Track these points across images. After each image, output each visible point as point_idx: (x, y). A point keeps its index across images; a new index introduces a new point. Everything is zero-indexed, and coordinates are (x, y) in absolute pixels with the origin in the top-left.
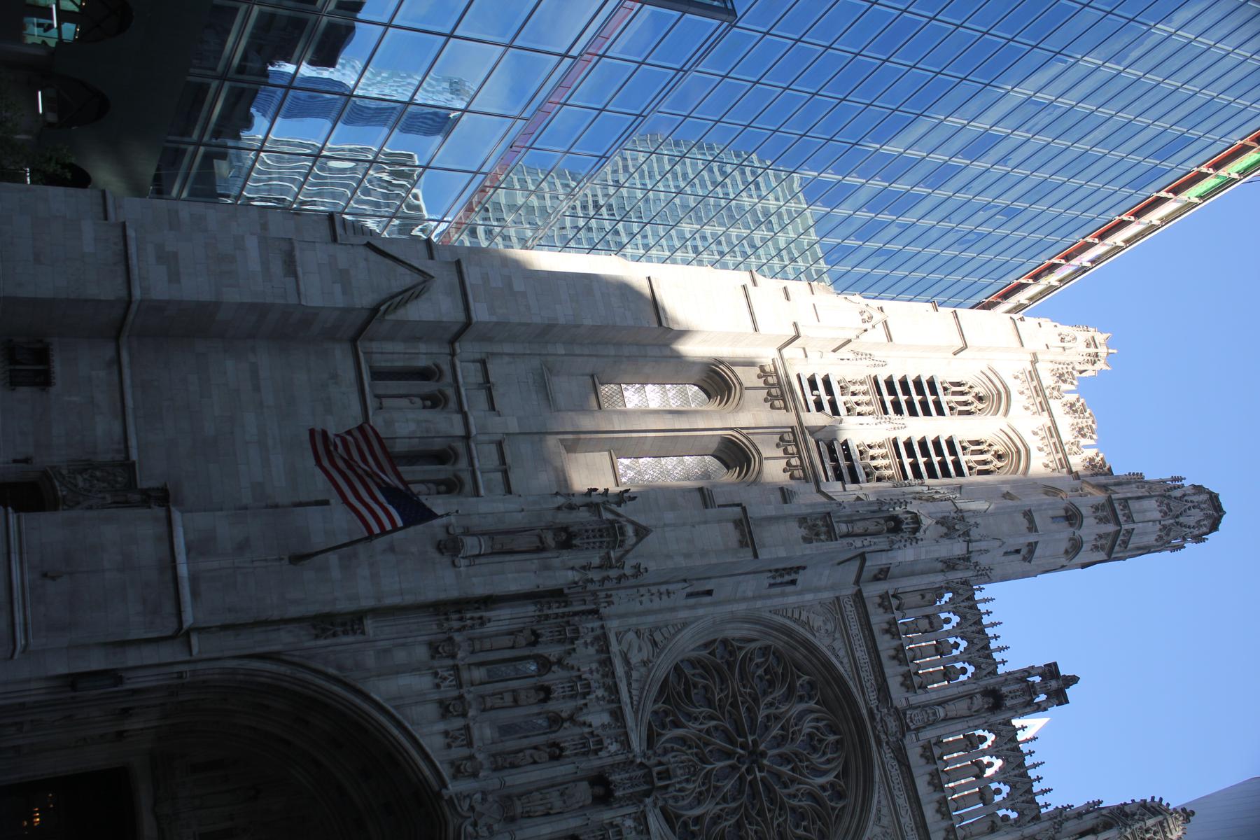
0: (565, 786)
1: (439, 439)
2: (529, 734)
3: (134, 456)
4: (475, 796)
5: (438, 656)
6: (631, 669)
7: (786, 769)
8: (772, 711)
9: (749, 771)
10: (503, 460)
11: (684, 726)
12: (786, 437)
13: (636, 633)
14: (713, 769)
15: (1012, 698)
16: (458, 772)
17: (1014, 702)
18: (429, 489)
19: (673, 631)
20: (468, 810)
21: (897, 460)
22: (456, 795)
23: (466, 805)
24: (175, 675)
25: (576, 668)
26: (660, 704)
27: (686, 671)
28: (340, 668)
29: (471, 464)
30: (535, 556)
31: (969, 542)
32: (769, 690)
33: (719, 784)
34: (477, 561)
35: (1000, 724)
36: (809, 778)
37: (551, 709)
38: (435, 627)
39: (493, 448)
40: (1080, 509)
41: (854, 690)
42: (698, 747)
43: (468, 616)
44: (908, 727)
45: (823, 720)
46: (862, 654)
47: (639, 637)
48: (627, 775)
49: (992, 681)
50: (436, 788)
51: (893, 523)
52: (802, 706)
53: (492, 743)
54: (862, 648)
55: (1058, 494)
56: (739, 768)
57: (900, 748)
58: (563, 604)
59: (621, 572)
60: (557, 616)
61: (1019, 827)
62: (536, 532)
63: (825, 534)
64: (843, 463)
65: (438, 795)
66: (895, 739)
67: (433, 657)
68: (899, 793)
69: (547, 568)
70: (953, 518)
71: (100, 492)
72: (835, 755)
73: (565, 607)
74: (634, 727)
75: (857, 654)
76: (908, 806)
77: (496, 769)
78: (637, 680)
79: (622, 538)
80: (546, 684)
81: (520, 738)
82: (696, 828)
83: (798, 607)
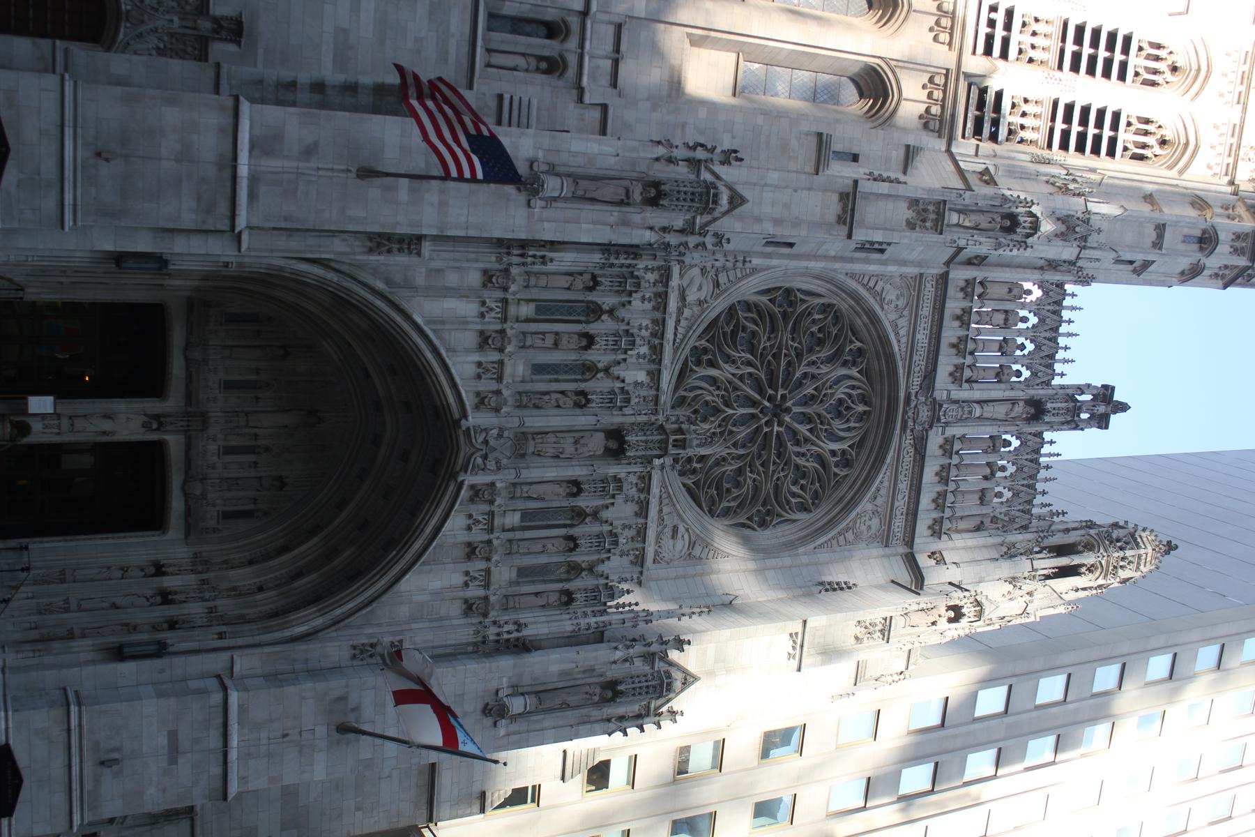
0: (582, 434)
1: (554, 10)
2: (561, 377)
4: (492, 432)
5: (489, 285)
6: (685, 306)
7: (803, 429)
8: (812, 370)
9: (767, 423)
10: (617, 49)
11: (719, 368)
12: (938, 80)
13: (702, 270)
14: (735, 414)
15: (1053, 414)
16: (481, 402)
17: (1053, 419)
18: (528, 64)
19: (739, 275)
20: (482, 442)
21: (1049, 124)
22: (474, 427)
23: (481, 438)
24: (222, 264)
25: (626, 320)
26: (703, 342)
27: (740, 313)
28: (388, 282)
29: (582, 46)
30: (617, 208)
31: (1084, 248)
32: (817, 349)
33: (734, 429)
34: (554, 204)
35: (1030, 434)
36: (824, 442)
37: (589, 358)
38: (493, 259)
39: (611, 30)
40: (1219, 233)
41: (901, 371)
42: (726, 390)
43: (531, 253)
44: (939, 420)
45: (859, 388)
46: (922, 338)
47: (703, 275)
48: (644, 438)
49: (1042, 392)
50: (456, 415)
51: (1009, 223)
52: (843, 371)
53: (522, 382)
54: (925, 332)
55: (1205, 209)
56: (760, 419)
57: (923, 438)
58: (632, 256)
59: (701, 239)
60: (622, 266)
61: (1005, 532)
62: (627, 183)
63: (932, 221)
64: (989, 115)
65: (457, 424)
66: (921, 429)
67: (485, 285)
68: (903, 479)
69: (625, 223)
70: (1078, 218)
71: (168, 12)
72: (857, 425)
73: (633, 259)
74: (669, 365)
75: (919, 336)
76: (907, 494)
77: (520, 406)
78: (687, 319)
79: (714, 206)
80: (592, 332)
81: (551, 381)
82: (698, 466)
83: (877, 275)
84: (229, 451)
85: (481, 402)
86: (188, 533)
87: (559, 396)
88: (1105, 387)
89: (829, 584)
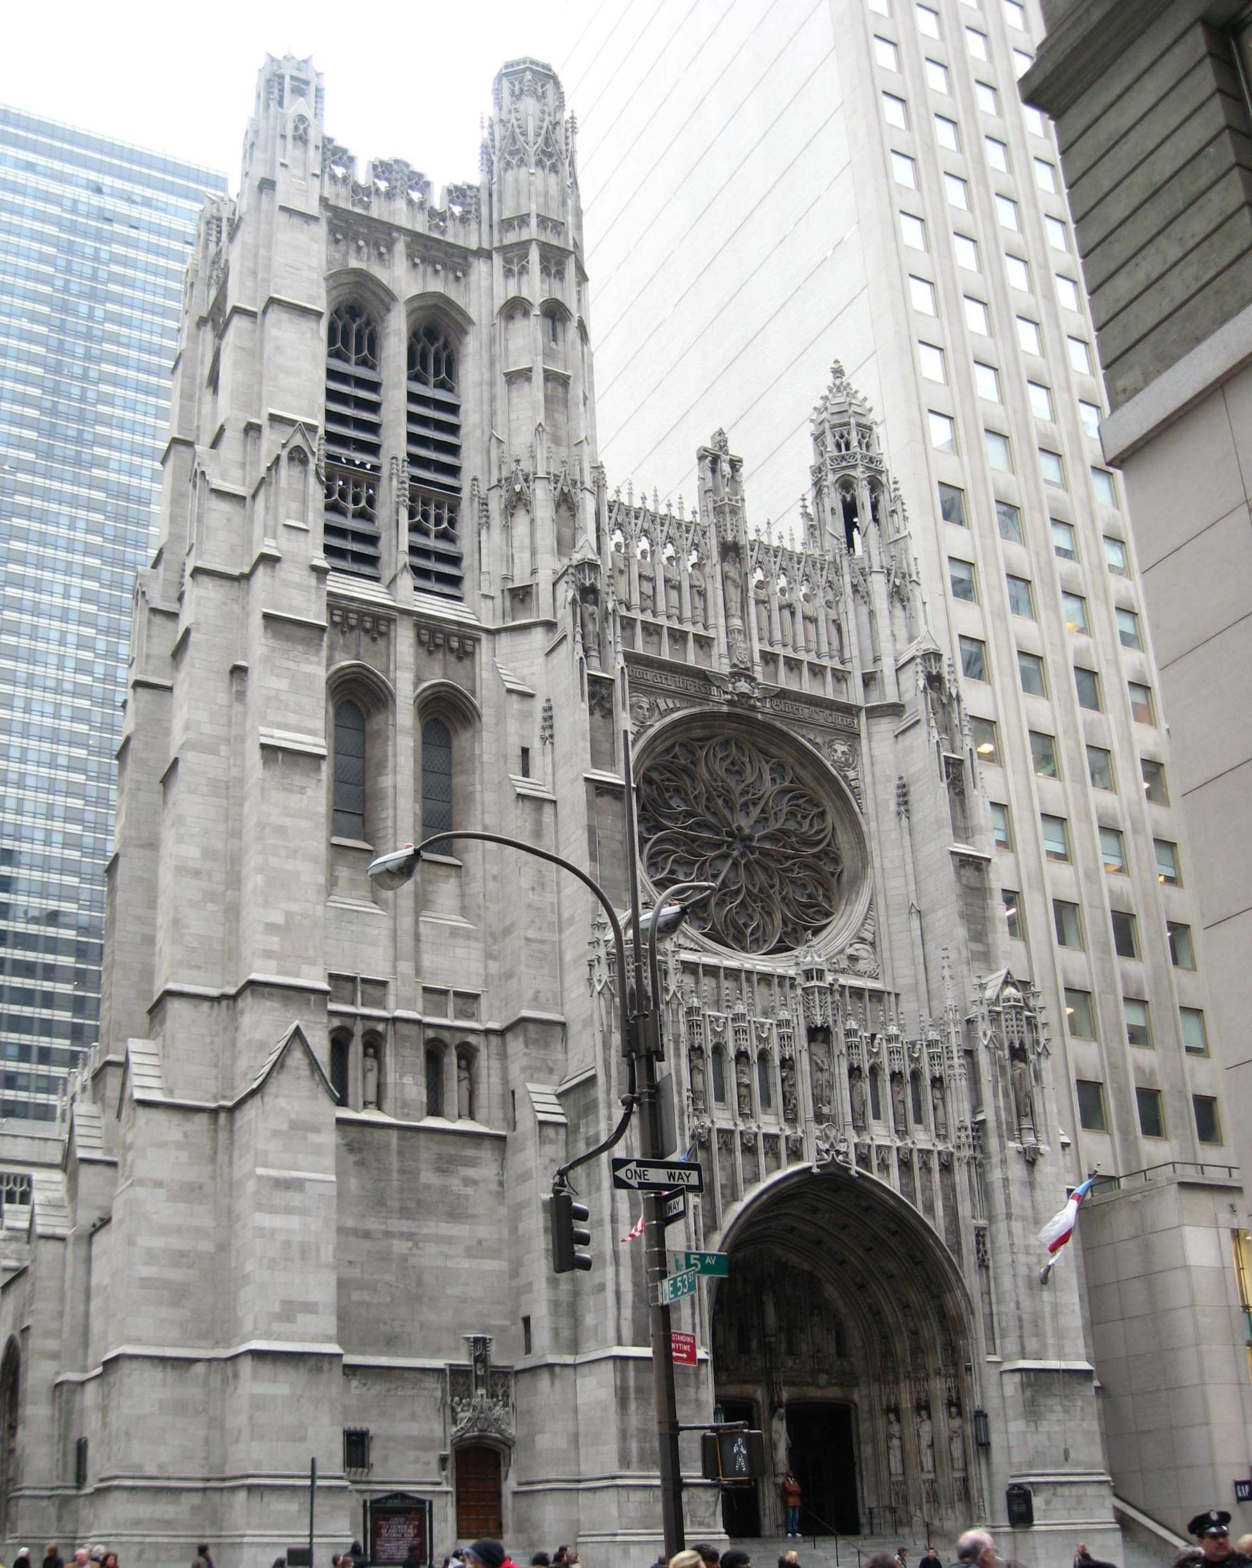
3: (439, 1363)
16: (796, 1155)
44: (747, 669)
46: (672, 683)
72: (747, 754)
85: (796, 1155)
87: (786, 1084)
88: (701, 458)
89: (899, 805)
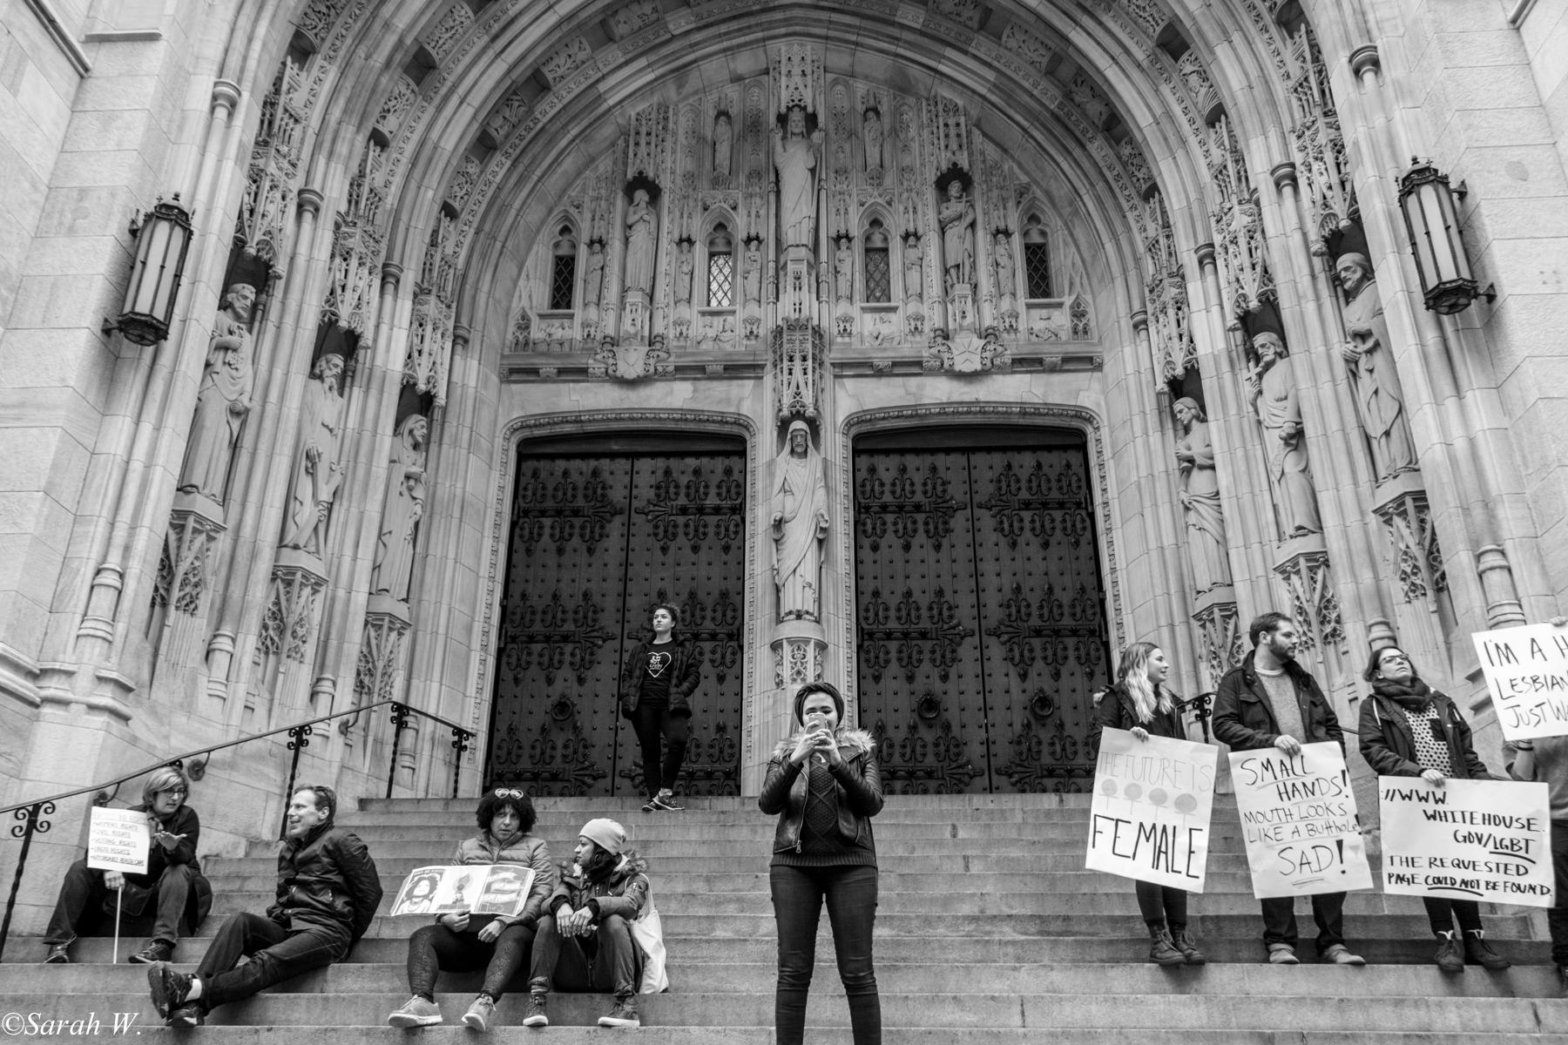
24: (221, 113)
84: (877, 290)
86: (1090, 363)
